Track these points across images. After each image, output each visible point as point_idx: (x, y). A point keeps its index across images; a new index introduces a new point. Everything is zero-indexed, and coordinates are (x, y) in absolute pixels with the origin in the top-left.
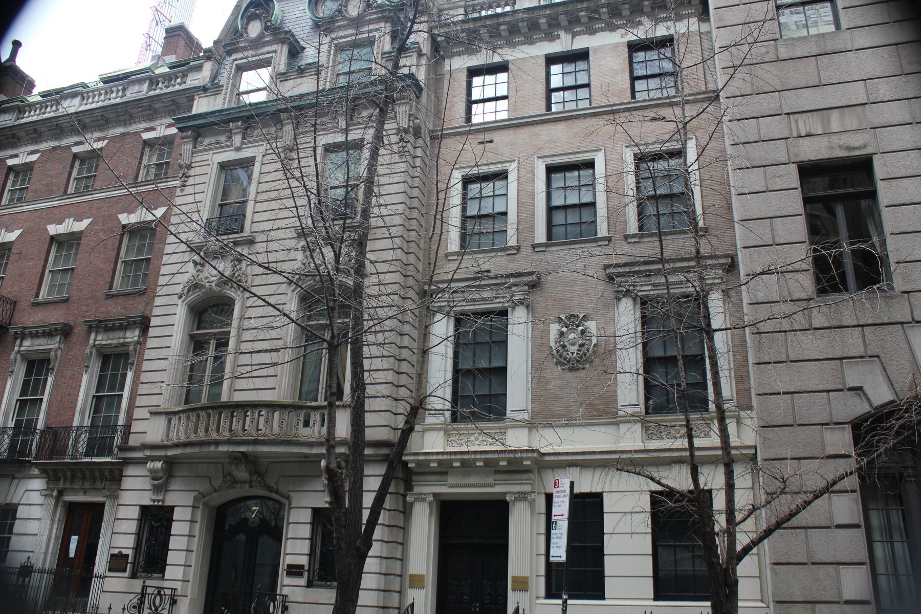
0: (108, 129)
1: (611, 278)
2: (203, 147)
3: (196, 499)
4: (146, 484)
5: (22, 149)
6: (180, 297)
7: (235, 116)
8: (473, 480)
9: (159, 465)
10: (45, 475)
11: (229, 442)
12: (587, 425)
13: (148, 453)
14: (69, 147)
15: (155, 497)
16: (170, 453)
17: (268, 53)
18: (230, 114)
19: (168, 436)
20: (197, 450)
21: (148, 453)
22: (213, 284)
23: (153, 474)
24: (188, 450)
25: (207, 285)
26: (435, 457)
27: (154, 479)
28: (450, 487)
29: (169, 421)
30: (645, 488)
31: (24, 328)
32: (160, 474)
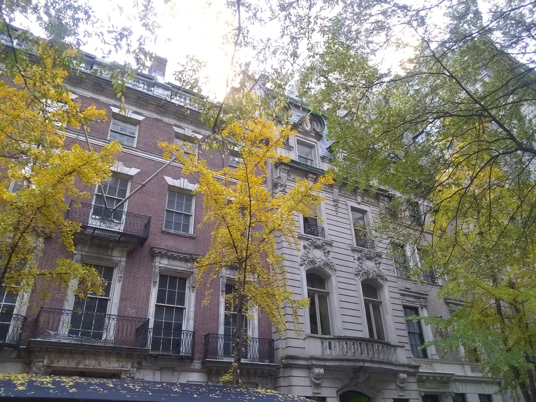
0: (182, 121)
1: (447, 304)
2: (291, 179)
3: (337, 392)
4: (307, 382)
5: (131, 107)
6: (302, 265)
7: (314, 172)
8: (434, 385)
9: (322, 371)
10: (203, 370)
11: (371, 361)
12: (454, 364)
13: (314, 362)
14: (170, 125)
15: (316, 391)
16: (328, 364)
17: (313, 142)
18: (312, 169)
19: (323, 353)
20: (352, 364)
21: (314, 362)
22: (322, 264)
23: (317, 377)
24: (345, 364)
25: (318, 263)
26: (425, 374)
27: (315, 379)
28: (426, 388)
29: (322, 342)
30: (476, 392)
31: (168, 251)
32: (320, 377)
